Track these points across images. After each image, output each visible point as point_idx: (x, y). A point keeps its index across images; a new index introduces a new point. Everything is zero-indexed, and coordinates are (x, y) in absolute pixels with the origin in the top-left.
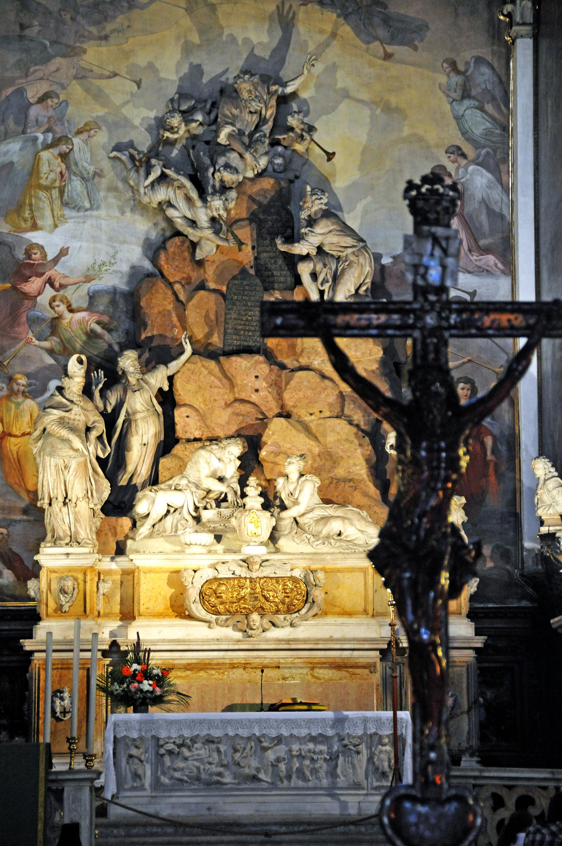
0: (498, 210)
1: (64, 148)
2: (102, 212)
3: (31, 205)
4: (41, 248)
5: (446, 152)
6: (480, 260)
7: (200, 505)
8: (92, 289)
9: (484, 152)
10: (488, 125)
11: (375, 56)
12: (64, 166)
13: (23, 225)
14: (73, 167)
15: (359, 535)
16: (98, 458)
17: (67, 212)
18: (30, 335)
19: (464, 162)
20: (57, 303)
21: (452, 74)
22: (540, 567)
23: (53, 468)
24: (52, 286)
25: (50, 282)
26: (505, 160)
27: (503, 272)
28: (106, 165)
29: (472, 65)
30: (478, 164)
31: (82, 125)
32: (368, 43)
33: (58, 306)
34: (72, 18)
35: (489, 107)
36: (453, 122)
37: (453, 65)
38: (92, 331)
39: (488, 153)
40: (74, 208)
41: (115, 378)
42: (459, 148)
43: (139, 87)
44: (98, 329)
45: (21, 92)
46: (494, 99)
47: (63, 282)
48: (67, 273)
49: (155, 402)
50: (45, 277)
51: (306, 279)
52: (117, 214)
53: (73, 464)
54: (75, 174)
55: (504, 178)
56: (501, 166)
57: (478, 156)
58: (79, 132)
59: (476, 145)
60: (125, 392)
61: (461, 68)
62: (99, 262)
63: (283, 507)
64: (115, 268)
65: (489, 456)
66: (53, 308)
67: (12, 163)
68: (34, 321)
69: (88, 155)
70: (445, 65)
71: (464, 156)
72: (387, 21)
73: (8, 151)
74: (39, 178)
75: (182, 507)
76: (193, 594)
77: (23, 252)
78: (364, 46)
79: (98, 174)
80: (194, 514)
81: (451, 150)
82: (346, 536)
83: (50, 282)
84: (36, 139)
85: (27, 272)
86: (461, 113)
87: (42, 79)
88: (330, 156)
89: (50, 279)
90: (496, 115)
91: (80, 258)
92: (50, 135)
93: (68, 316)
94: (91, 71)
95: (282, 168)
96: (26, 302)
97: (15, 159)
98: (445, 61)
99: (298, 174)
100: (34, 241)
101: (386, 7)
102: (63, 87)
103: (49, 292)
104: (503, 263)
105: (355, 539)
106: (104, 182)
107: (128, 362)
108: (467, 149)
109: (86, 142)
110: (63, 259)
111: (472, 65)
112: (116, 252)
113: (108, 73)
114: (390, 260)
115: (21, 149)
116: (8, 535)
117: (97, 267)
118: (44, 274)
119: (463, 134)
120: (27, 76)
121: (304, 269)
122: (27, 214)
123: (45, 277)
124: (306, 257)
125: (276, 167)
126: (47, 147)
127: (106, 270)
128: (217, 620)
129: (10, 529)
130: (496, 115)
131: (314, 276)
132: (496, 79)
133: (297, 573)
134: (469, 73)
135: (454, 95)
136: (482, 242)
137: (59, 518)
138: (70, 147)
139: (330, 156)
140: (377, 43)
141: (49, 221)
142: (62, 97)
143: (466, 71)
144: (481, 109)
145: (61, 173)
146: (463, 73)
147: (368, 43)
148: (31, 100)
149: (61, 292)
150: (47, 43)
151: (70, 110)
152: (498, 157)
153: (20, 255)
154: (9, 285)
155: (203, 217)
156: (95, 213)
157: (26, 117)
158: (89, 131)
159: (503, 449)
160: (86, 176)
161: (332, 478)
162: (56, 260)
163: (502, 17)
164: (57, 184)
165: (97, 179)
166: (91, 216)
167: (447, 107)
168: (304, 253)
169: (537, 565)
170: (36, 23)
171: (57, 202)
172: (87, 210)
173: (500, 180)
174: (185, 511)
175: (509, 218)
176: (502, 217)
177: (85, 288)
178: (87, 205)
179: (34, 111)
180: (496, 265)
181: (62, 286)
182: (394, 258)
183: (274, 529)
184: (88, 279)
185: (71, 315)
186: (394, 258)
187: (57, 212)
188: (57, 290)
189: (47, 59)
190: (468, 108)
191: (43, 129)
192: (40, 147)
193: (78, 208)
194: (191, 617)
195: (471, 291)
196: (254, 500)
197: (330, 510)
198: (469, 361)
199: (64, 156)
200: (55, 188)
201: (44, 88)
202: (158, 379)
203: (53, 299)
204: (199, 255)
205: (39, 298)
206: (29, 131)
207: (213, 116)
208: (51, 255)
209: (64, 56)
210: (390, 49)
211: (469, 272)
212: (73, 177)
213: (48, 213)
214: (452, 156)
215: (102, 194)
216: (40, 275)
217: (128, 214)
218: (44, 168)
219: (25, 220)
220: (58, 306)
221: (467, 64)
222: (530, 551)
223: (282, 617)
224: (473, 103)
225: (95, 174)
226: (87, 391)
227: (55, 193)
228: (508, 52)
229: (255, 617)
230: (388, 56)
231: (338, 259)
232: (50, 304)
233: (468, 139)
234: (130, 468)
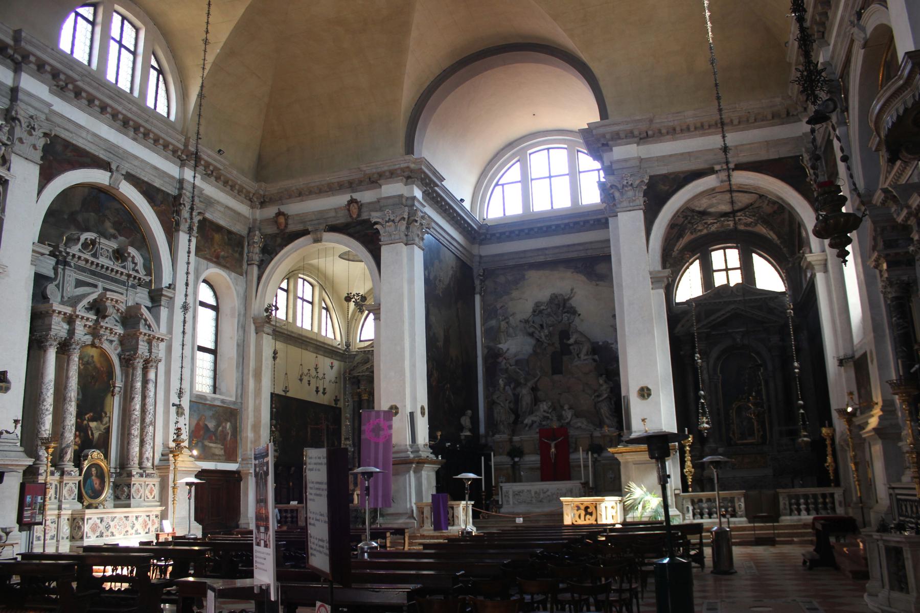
16: (511, 409)
91: (513, 350)
103: (505, 361)
124: (571, 345)
179: (499, 311)
208: (505, 350)
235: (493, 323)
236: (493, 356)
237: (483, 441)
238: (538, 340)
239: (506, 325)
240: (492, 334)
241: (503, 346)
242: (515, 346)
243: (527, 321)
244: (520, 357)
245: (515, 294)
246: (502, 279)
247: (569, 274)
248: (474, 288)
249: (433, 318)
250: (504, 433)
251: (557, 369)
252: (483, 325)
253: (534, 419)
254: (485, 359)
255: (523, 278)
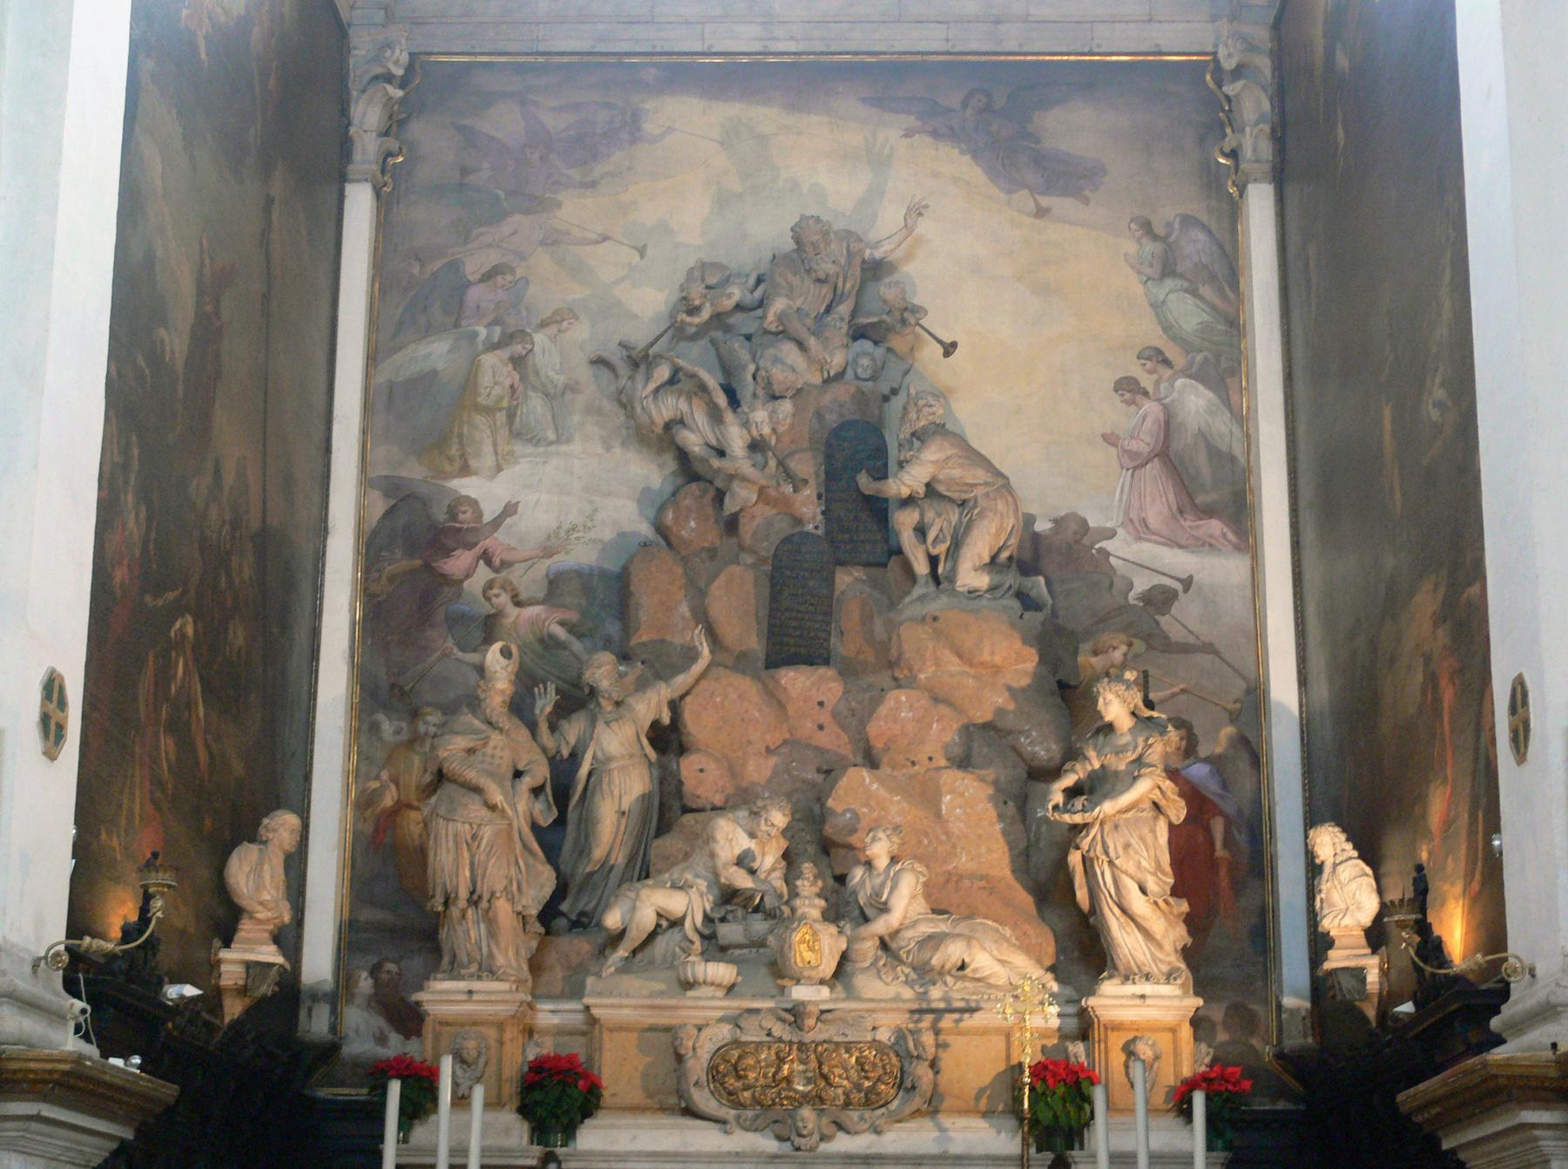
0: (1225, 449)
1: (518, 349)
2: (576, 447)
3: (460, 436)
4: (474, 503)
5: (1139, 358)
6: (1198, 527)
7: (717, 915)
8: (553, 570)
9: (1199, 358)
10: (1206, 317)
11: (1020, 211)
12: (517, 377)
13: (447, 468)
14: (532, 378)
15: (997, 968)
16: (535, 827)
17: (518, 447)
18: (450, 643)
19: (1167, 373)
20: (495, 591)
21: (1144, 240)
22: (1310, 1040)
23: (451, 838)
24: (489, 563)
25: (486, 557)
26: (1234, 371)
27: (1237, 548)
28: (584, 374)
29: (1177, 226)
30: (1190, 377)
31: (548, 314)
32: (1010, 192)
33: (497, 596)
34: (541, 158)
35: (1206, 291)
36: (1149, 309)
37: (1147, 227)
38: (551, 636)
39: (1206, 360)
40: (530, 441)
41: (577, 699)
42: (1159, 352)
43: (642, 257)
44: (561, 633)
45: (455, 266)
46: (1213, 278)
47: (508, 557)
48: (513, 543)
49: (645, 742)
50: (478, 550)
51: (907, 539)
52: (600, 450)
53: (487, 833)
54: (534, 388)
55: (1234, 398)
56: (1229, 381)
57: (1190, 364)
58: (543, 325)
59: (1186, 346)
60: (593, 722)
61: (1160, 230)
62: (566, 526)
63: (866, 920)
64: (593, 535)
65: (1220, 851)
66: (488, 599)
67: (435, 373)
68: (457, 621)
69: (556, 360)
70: (1133, 226)
71: (1166, 362)
72: (1040, 160)
73: (429, 355)
74: (476, 394)
75: (684, 917)
76: (697, 1067)
77: (445, 509)
78: (1002, 196)
79: (572, 388)
80: (706, 932)
81: (1147, 354)
82: (975, 971)
83: (486, 557)
84: (475, 335)
85: (450, 543)
86: (1162, 297)
87: (489, 246)
88: (949, 349)
89: (485, 552)
90: (1217, 301)
92: (498, 330)
93: (513, 612)
94: (568, 233)
95: (869, 372)
96: (446, 589)
97: (440, 365)
98: (1132, 220)
99: (896, 386)
100: (464, 492)
101: (1038, 142)
102: (523, 258)
103: (483, 574)
104: (1236, 533)
105: (990, 976)
106: (581, 400)
107: (602, 671)
108: (1172, 352)
109: (553, 339)
110: (508, 520)
111: (1177, 226)
112: (596, 510)
113: (594, 236)
114: (1049, 525)
115: (450, 351)
116: (399, 974)
117: (562, 533)
118: (476, 544)
119: (1165, 330)
120: (466, 242)
121: (904, 522)
122: (454, 450)
123: (478, 550)
124: (909, 502)
125: (860, 371)
126: (492, 347)
127: (578, 539)
128: (738, 1118)
129: (403, 963)
130: (1217, 301)
131: (921, 531)
132: (1215, 248)
133: (884, 1036)
134: (1172, 239)
135: (1149, 271)
136: (1200, 499)
137: (467, 933)
138: (529, 347)
139: (949, 349)
140: (1025, 192)
141: (489, 461)
142: (519, 272)
143: (1168, 236)
144: (1194, 293)
145: (512, 386)
146: (1163, 239)
147: (1010, 192)
148: (471, 278)
149: (504, 574)
150: (501, 194)
151: (532, 291)
152: (1224, 365)
153: (440, 515)
154: (418, 562)
155: (736, 439)
156: (564, 448)
157: (461, 302)
158: (559, 322)
159: (1242, 839)
160: (552, 391)
161: (949, 873)
162: (497, 523)
163: (1222, 161)
164: (505, 404)
165: (568, 396)
166: (557, 453)
167: (1140, 289)
168: (905, 492)
169: (1305, 1037)
170: (486, 165)
171: (503, 433)
172: (551, 443)
173: (1227, 402)
174: (688, 924)
175: (1242, 460)
176: (1232, 459)
177: (544, 566)
178: (551, 435)
179: (475, 294)
180: (1224, 535)
181: (505, 564)
182: (1055, 521)
183: (844, 958)
184: (548, 553)
185: (517, 611)
186: (1055, 521)
187: (503, 448)
188: (497, 571)
189: (498, 216)
190: (1171, 291)
191: (486, 321)
192: (481, 348)
193: (536, 441)
194: (690, 1112)
195: (1184, 576)
196: (810, 905)
197: (942, 926)
198: (1183, 691)
199: (518, 362)
200: (501, 409)
201: (493, 258)
202: (650, 706)
203: (490, 585)
204: (730, 506)
205: (466, 584)
206: (464, 323)
207: (758, 294)
208: (490, 511)
209: (527, 212)
210: (1044, 201)
211: (1181, 547)
212: (531, 393)
213: (488, 448)
214: (1149, 363)
215: (576, 418)
216: (470, 546)
217: (618, 450)
218: (486, 380)
219: (451, 460)
220: (497, 596)
221: (1169, 225)
222: (1293, 1012)
223: (855, 1115)
224: (1179, 283)
225: (567, 387)
226: (520, 707)
227: (501, 417)
228: (1233, 212)
229: (806, 1112)
230: (1041, 212)
231: (963, 504)
232: (484, 592)
233: (1173, 338)
234: (598, 853)
235: (436, 353)
236: (419, 550)
237: (317, 1024)
238: (688, 469)
239: (508, 375)
240: (423, 419)
241: (483, 490)
242: (557, 494)
243: (640, 361)
244: (582, 555)
245: (573, 210)
246: (504, 123)
247: (891, 133)
248: (345, 147)
249: (150, 151)
250: (488, 970)
251: (793, 638)
252: (373, 359)
253: (676, 903)
254: (371, 549)
255: (630, 128)
